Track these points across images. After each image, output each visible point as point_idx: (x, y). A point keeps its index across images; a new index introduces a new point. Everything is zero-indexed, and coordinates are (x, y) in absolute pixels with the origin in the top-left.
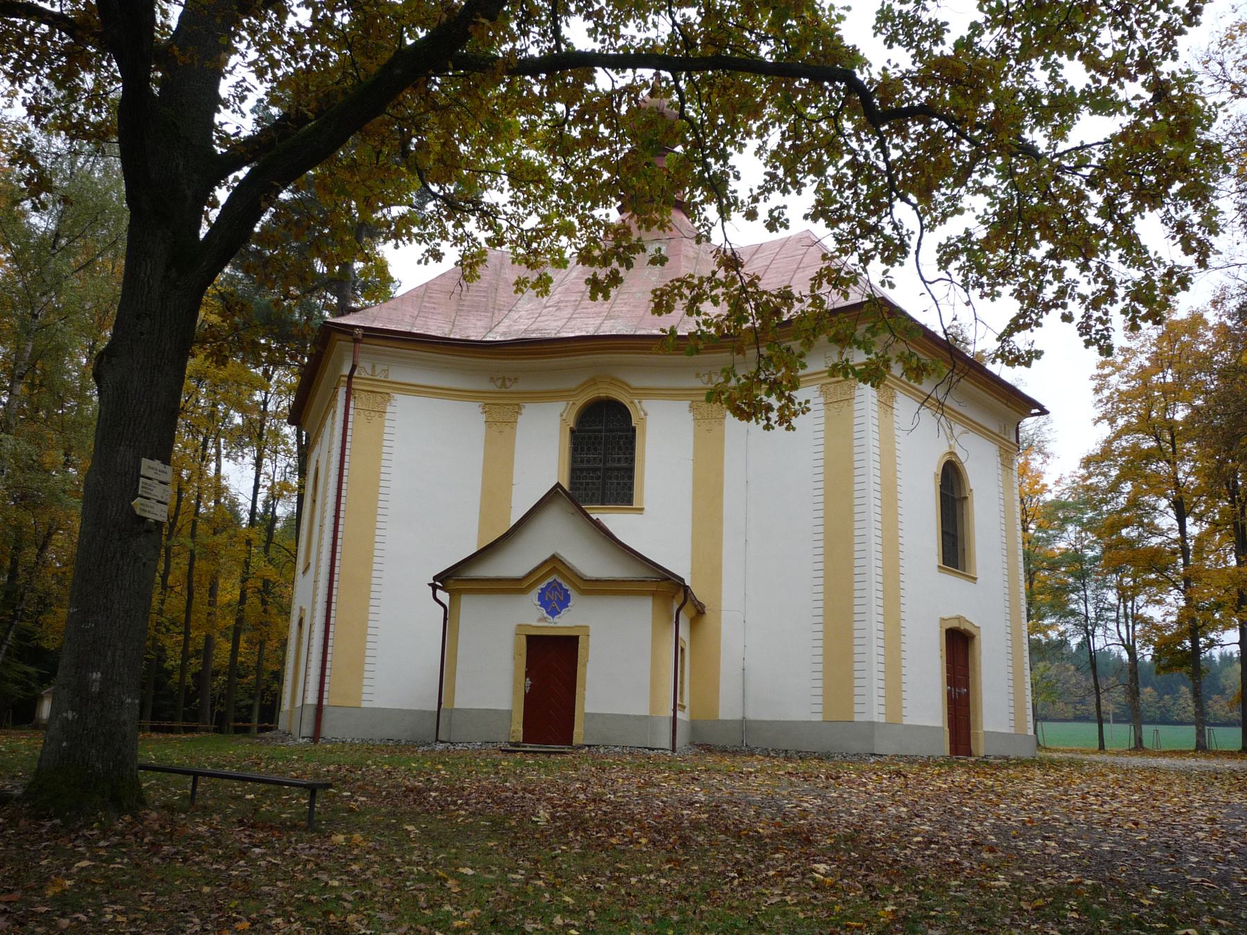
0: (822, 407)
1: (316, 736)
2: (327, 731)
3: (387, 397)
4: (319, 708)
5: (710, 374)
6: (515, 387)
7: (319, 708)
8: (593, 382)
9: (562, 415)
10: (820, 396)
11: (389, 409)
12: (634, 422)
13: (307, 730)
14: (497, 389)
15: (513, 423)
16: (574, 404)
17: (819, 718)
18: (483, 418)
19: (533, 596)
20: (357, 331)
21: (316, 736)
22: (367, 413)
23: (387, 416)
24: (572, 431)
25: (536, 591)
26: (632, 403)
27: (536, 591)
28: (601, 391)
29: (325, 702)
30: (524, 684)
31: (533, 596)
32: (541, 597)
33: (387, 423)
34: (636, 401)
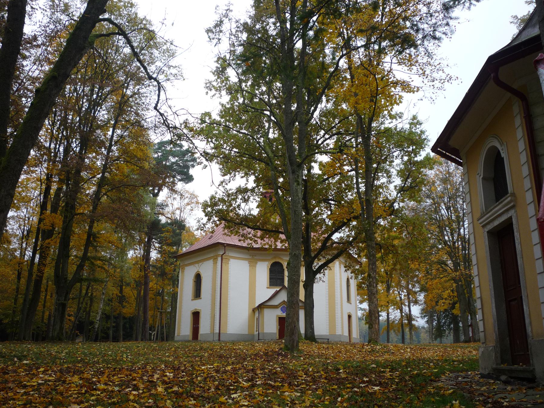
1: (219, 340)
2: (221, 339)
3: (229, 260)
4: (219, 333)
6: (255, 258)
7: (219, 333)
8: (275, 258)
13: (217, 339)
17: (328, 334)
19: (280, 309)
20: (225, 245)
21: (219, 340)
25: (280, 309)
27: (280, 309)
30: (278, 327)
31: (280, 309)
32: (281, 309)
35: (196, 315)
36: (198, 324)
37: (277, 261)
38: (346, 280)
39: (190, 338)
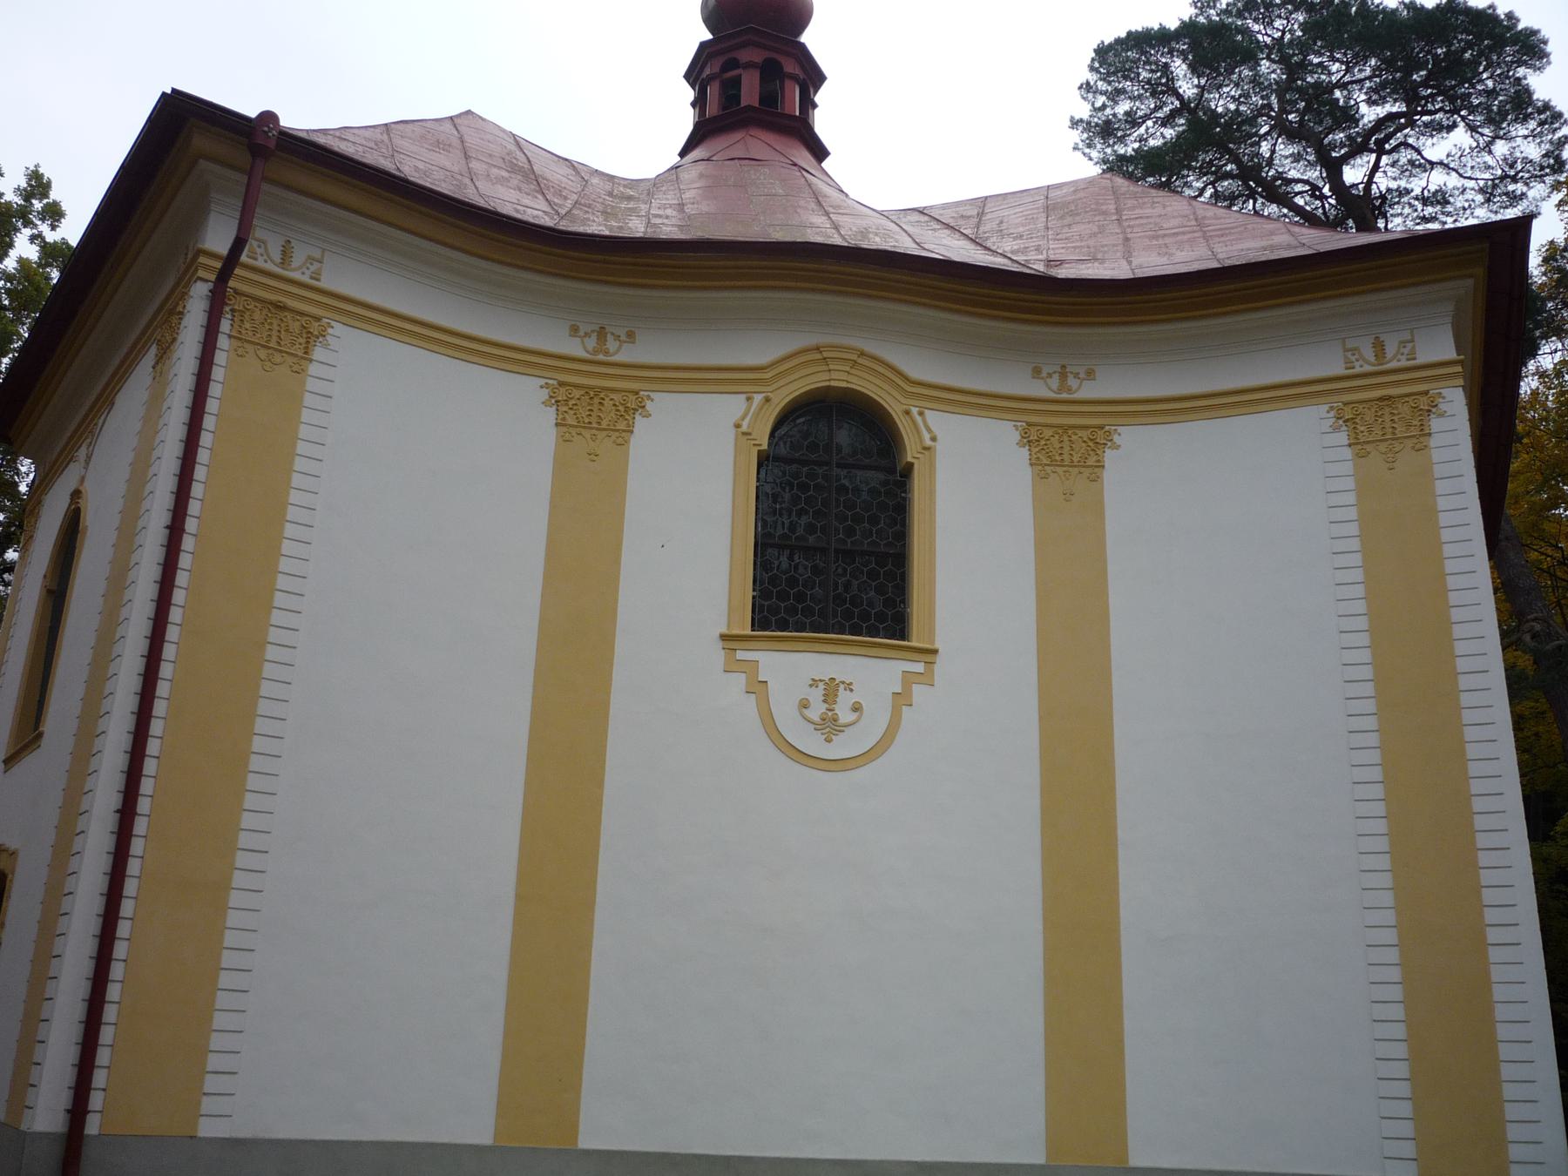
0: (1348, 453)
5: (1063, 376)
9: (738, 426)
10: (1336, 429)
11: (318, 353)
14: (580, 353)
16: (767, 400)
18: (550, 414)
22: (263, 353)
23: (313, 369)
24: (764, 460)
26: (907, 413)
28: (834, 375)
29: (93, 1126)
33: (311, 384)
34: (915, 411)
37: (841, 378)
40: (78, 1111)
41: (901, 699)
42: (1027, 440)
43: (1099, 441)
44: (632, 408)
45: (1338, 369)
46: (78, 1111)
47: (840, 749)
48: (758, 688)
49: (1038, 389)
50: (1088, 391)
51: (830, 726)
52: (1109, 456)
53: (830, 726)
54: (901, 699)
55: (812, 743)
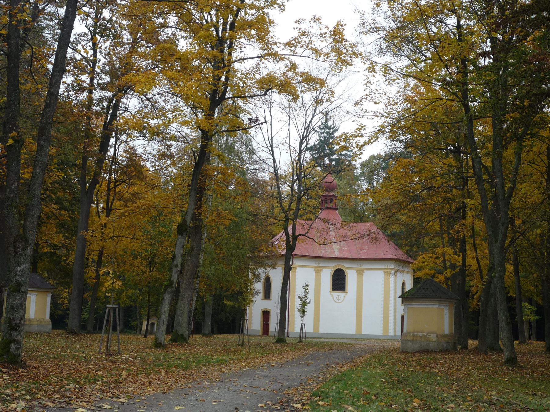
12: (346, 274)
15: (320, 273)
35: (266, 314)
36: (269, 321)
38: (401, 285)
39: (261, 333)
40: (288, 330)
41: (345, 297)
42: (357, 272)
43: (363, 272)
44: (321, 270)
45: (383, 267)
46: (288, 330)
47: (339, 301)
48: (333, 296)
49: (358, 267)
50: (363, 267)
51: (339, 299)
52: (364, 273)
53: (339, 299)
54: (345, 297)
55: (337, 301)
